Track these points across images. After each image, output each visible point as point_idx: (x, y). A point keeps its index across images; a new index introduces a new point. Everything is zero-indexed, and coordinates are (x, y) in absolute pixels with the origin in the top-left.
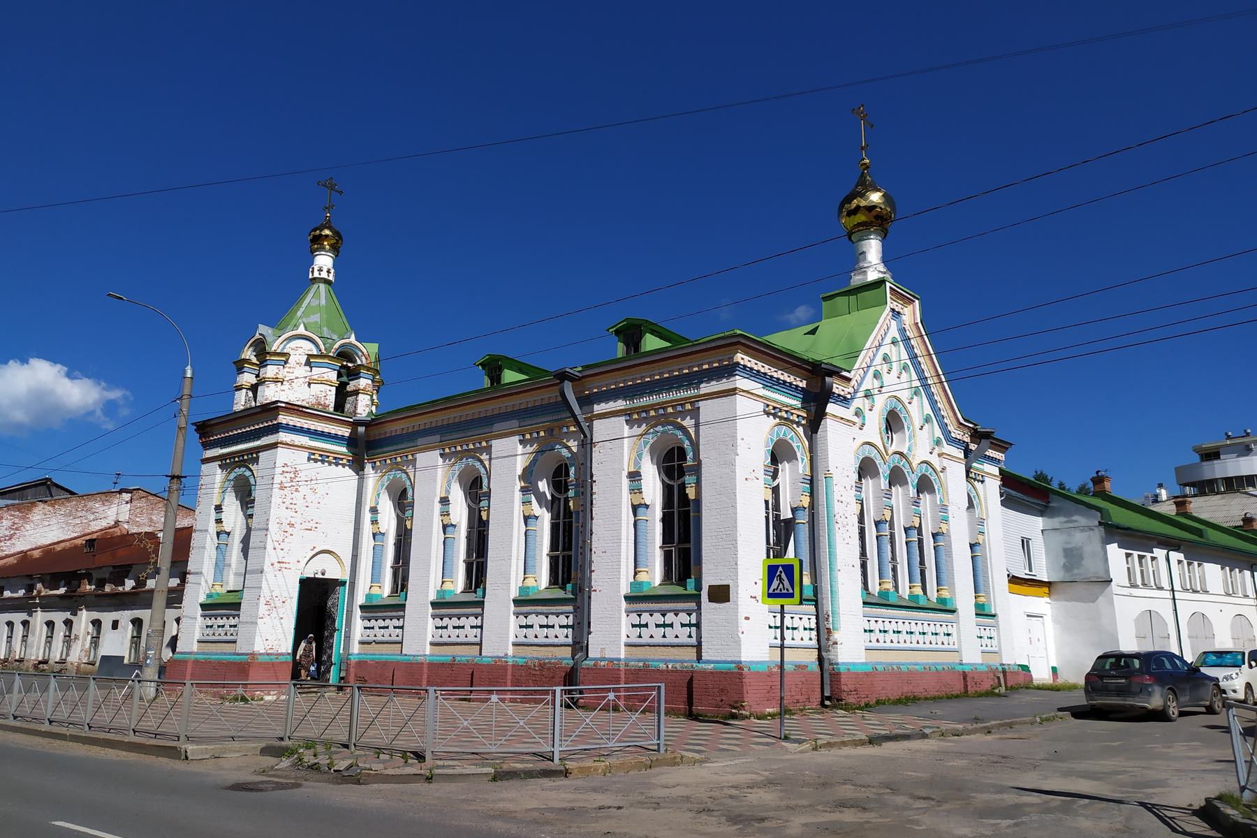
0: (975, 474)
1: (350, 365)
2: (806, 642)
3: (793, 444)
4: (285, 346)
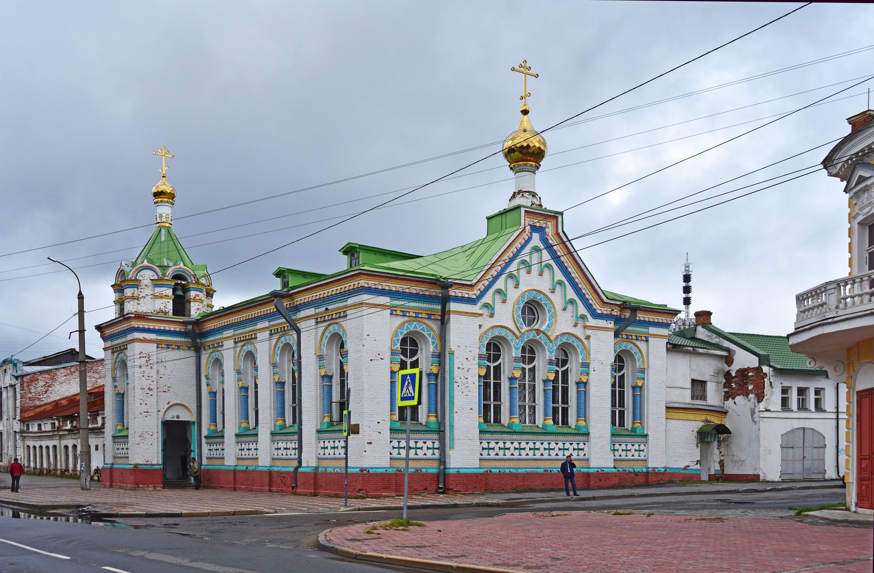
1: (183, 282)
3: (424, 333)
4: (137, 274)
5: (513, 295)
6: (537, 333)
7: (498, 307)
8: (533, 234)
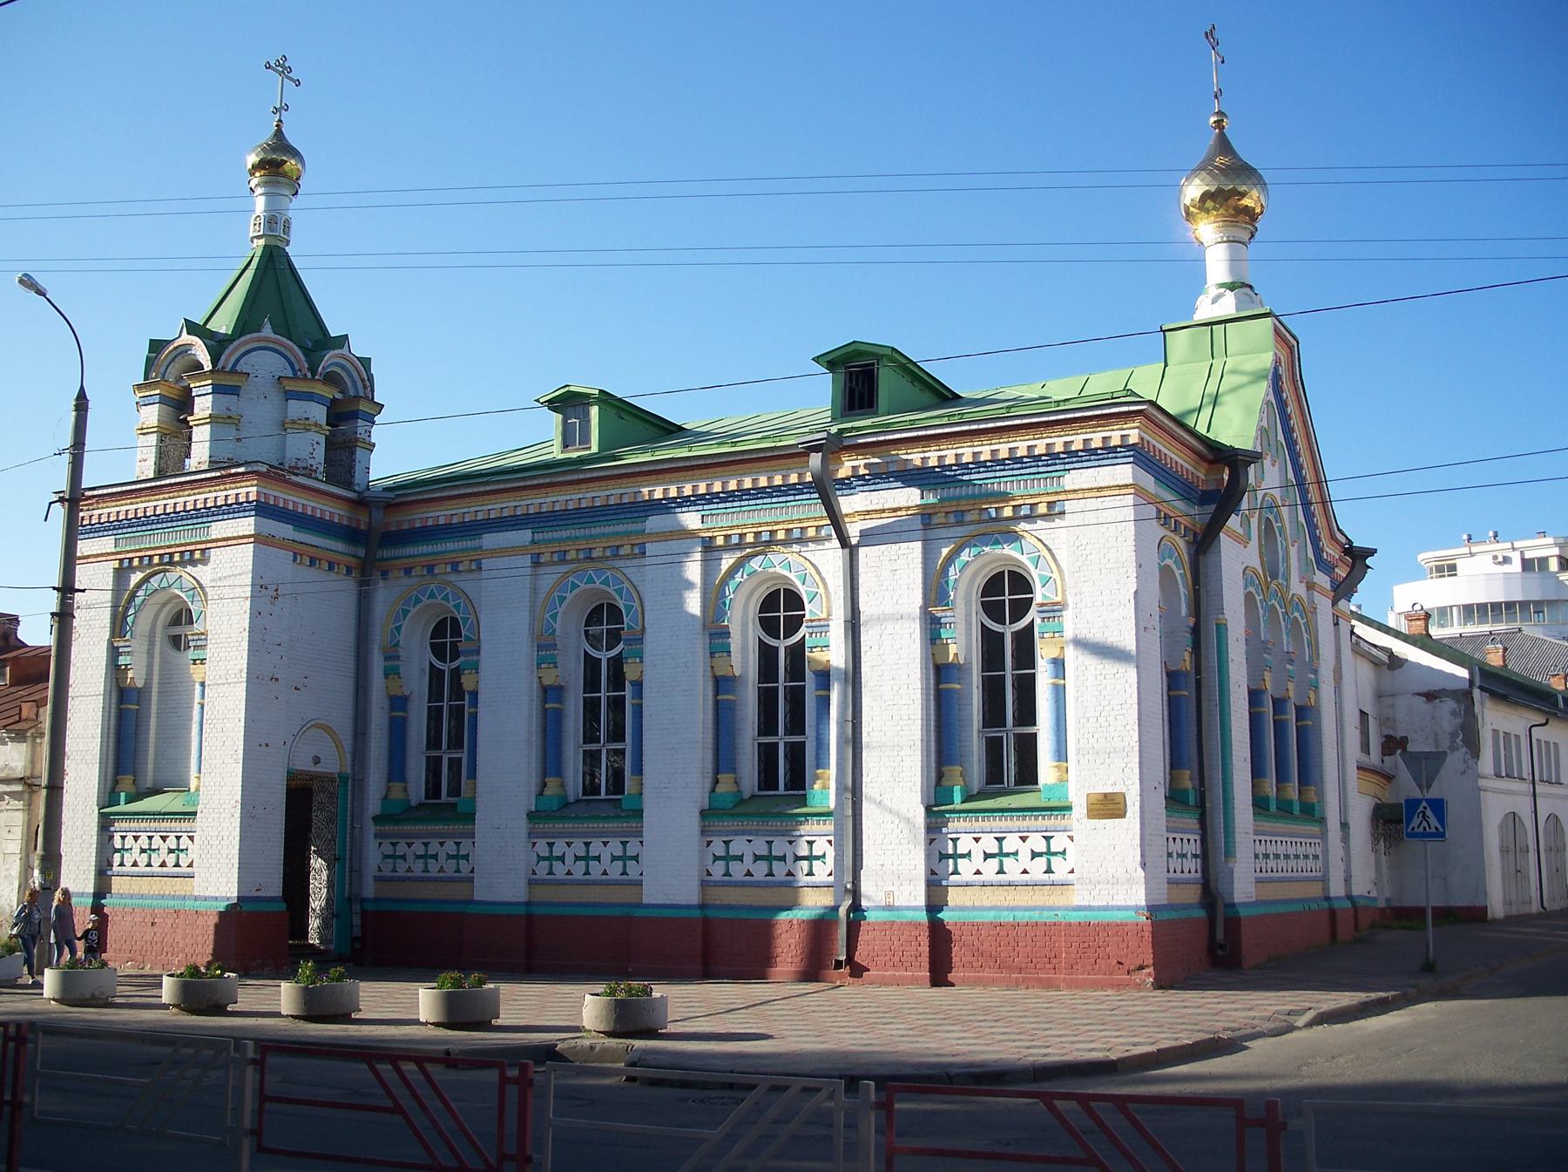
2: (1193, 875)
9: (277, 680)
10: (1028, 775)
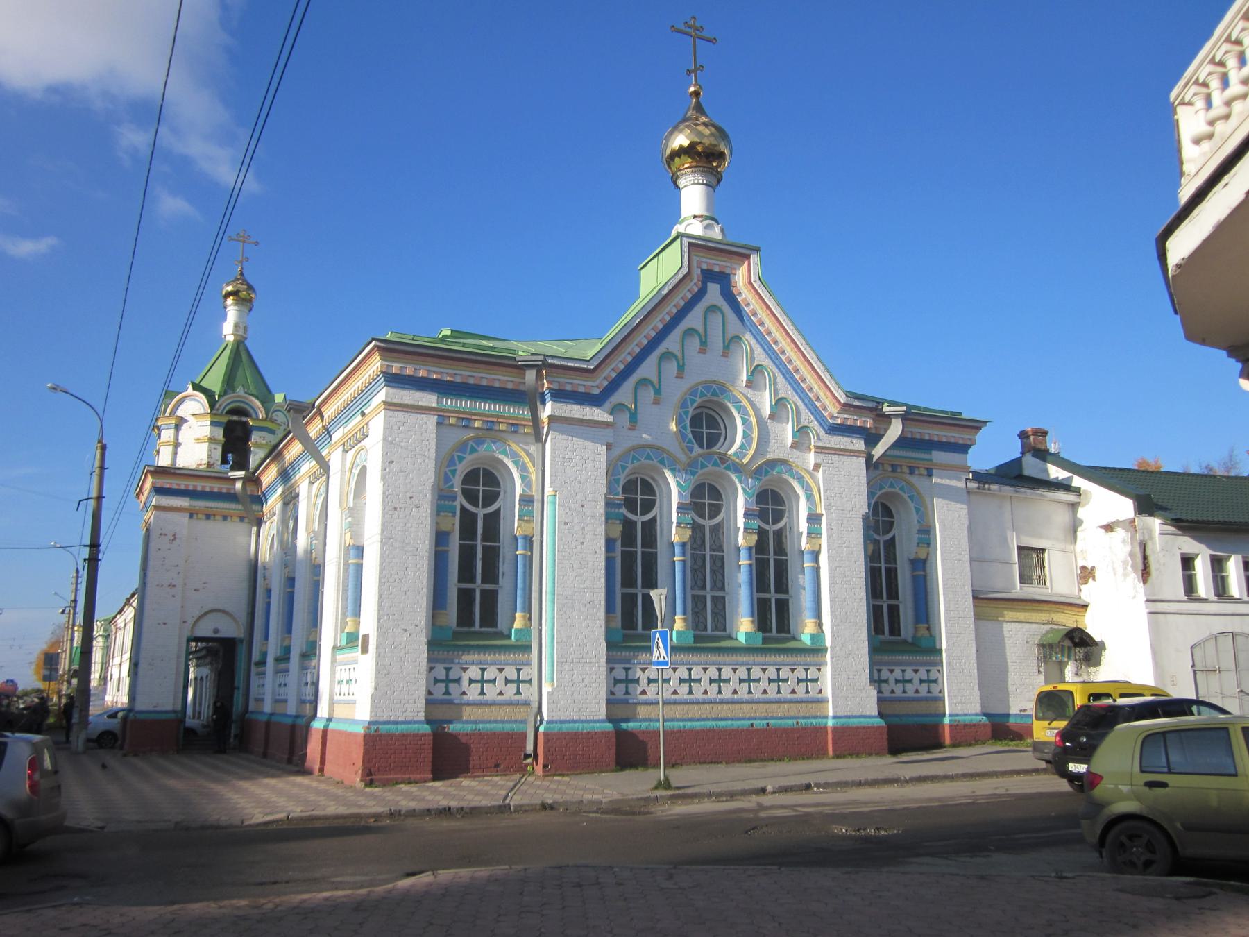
0: (910, 468)
5: (676, 390)
6: (720, 458)
7: (648, 410)
8: (709, 284)
9: (174, 586)
10: (490, 616)
